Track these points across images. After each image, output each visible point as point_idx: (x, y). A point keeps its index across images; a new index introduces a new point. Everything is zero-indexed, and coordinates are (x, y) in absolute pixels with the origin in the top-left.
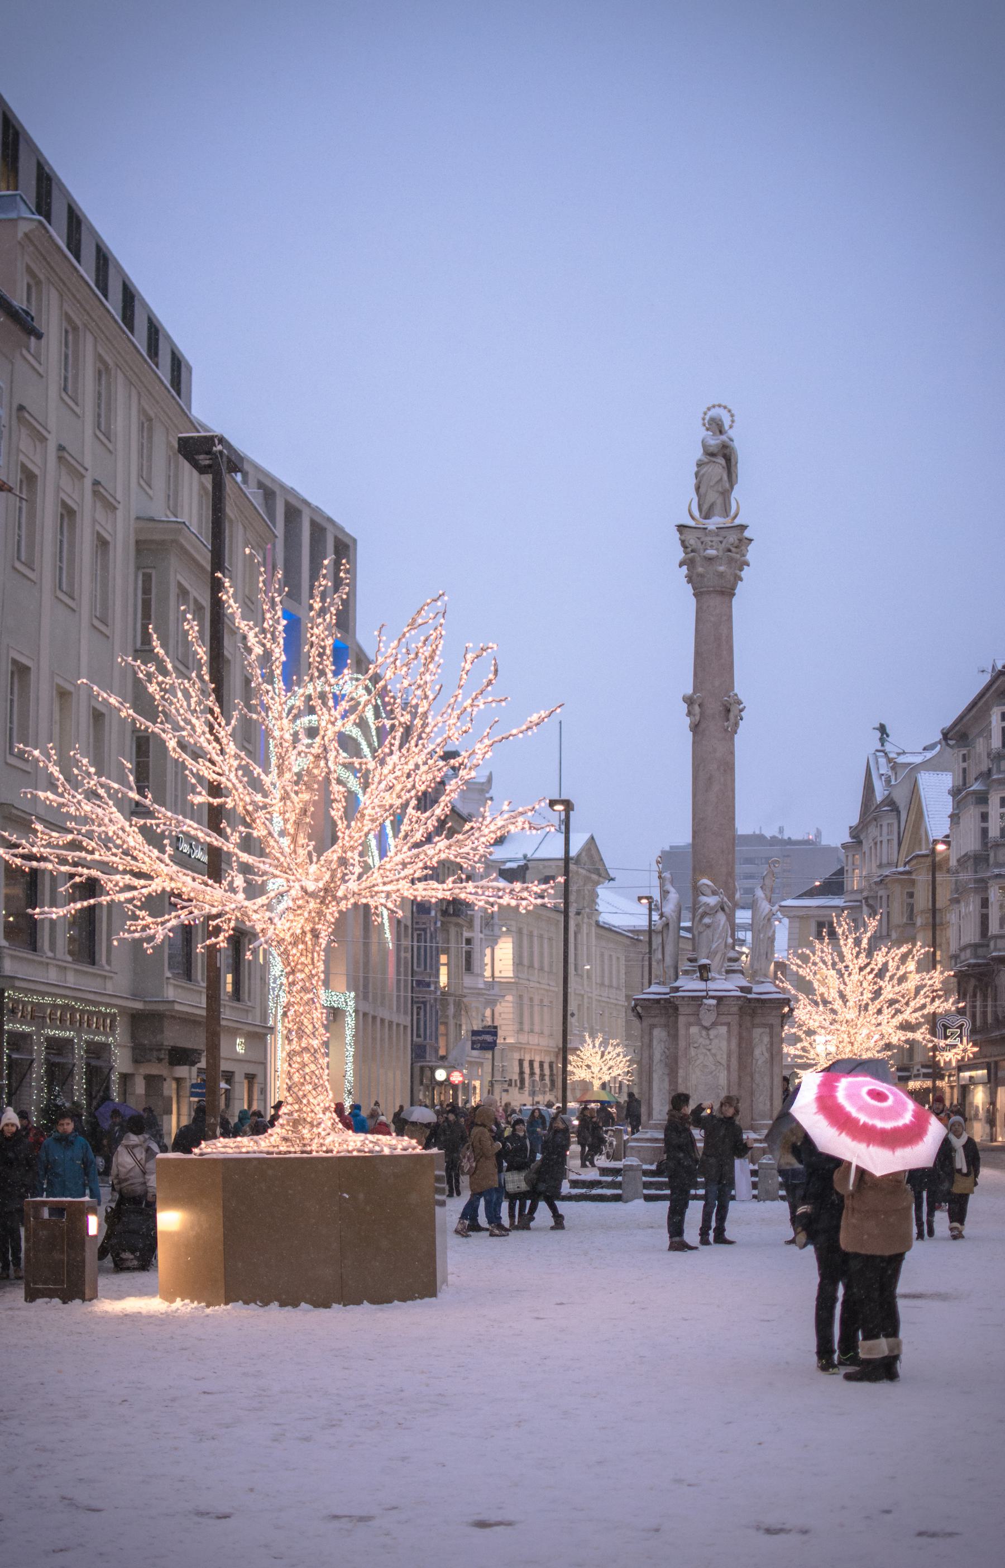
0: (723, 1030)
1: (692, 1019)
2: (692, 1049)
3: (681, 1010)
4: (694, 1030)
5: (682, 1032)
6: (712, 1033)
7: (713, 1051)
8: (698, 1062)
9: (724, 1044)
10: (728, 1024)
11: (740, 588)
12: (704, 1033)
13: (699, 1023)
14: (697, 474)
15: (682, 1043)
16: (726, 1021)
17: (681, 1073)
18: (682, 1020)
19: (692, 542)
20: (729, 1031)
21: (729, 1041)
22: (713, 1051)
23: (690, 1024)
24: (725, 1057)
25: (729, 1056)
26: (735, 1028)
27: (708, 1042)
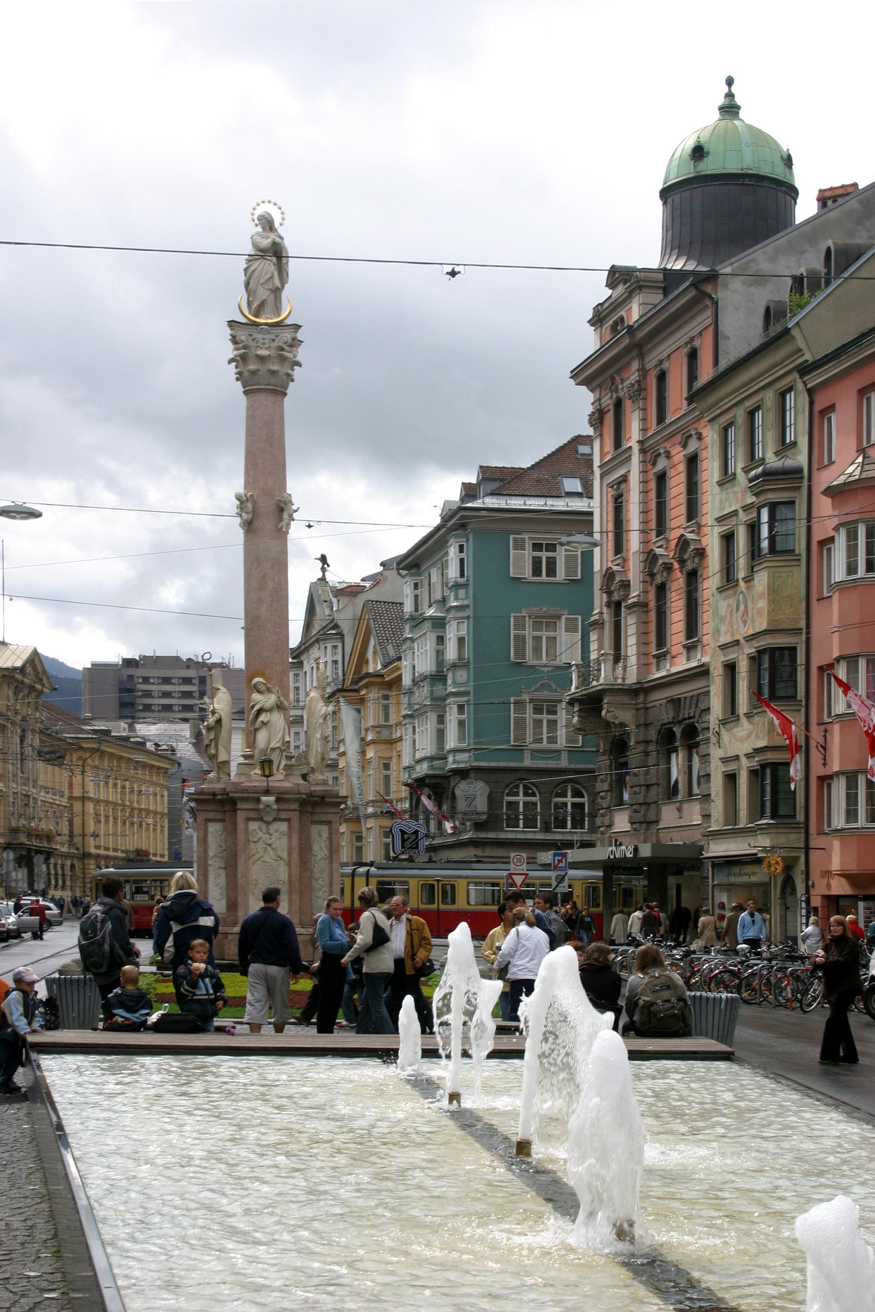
0: (284, 826)
1: (252, 815)
2: (252, 845)
3: (239, 806)
4: (253, 826)
5: (241, 826)
9: (285, 840)
10: (288, 820)
12: (264, 827)
13: (261, 819)
15: (241, 837)
17: (241, 869)
18: (241, 816)
20: (290, 828)
21: (290, 838)
23: (249, 819)
25: (290, 854)
26: (296, 824)
27: (267, 836)
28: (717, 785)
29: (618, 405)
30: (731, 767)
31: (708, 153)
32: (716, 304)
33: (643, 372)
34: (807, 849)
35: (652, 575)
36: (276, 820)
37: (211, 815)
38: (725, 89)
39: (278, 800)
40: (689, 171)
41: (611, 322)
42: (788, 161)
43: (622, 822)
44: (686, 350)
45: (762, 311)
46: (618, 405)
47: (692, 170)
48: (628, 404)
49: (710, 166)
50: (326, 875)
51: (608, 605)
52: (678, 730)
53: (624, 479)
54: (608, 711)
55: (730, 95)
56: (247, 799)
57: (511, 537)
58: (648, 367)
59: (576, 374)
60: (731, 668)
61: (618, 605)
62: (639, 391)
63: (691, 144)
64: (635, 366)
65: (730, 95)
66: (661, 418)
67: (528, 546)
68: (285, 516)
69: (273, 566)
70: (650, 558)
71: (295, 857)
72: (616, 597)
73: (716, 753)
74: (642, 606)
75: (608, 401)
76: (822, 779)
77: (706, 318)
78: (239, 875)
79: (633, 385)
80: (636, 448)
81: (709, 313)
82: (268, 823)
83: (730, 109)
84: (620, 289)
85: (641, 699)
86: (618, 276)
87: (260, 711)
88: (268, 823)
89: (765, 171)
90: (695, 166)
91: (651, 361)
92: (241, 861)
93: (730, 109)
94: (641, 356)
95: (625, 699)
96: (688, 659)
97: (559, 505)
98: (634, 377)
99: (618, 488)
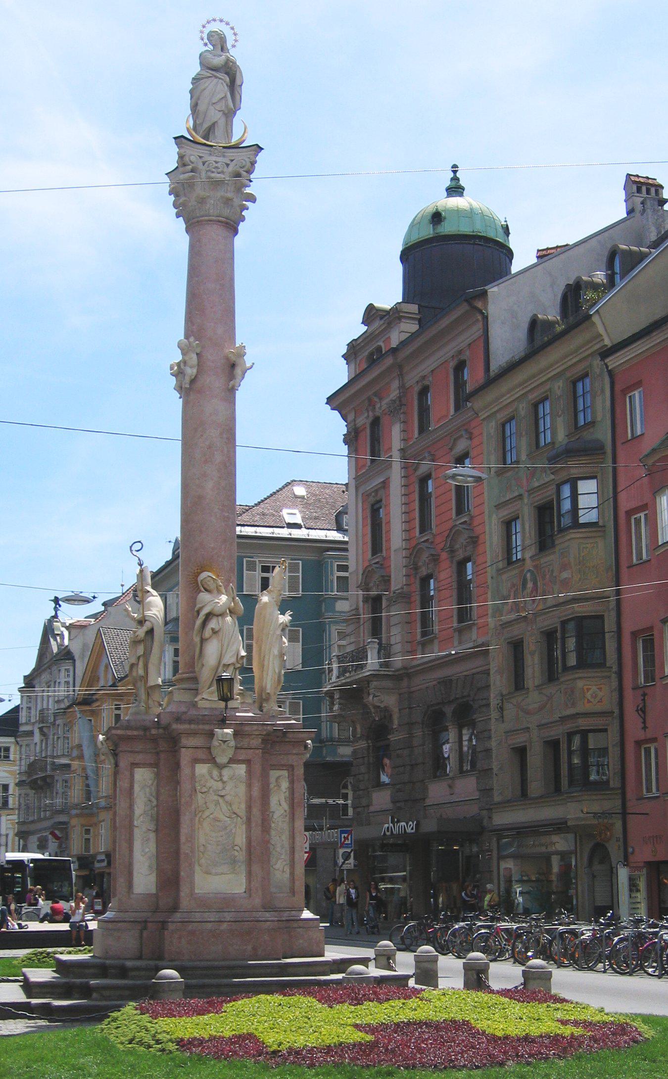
0: (241, 769)
1: (201, 754)
2: (199, 795)
3: (184, 741)
4: (202, 769)
5: (185, 771)
6: (226, 773)
7: (228, 798)
8: (207, 813)
9: (242, 789)
10: (248, 762)
11: (242, 227)
12: (215, 773)
13: (212, 760)
14: (191, 92)
15: (186, 786)
16: (248, 757)
17: (184, 830)
18: (185, 756)
19: (193, 158)
20: (249, 772)
21: (249, 786)
22: (228, 798)
23: (196, 761)
24: (243, 806)
25: (249, 808)
26: (257, 768)
27: (220, 784)
28: (500, 759)
29: (376, 423)
30: (520, 739)
31: (445, 218)
32: (486, 318)
33: (404, 390)
34: (624, 814)
35: (416, 568)
36: (232, 761)
37: (139, 758)
38: (452, 175)
39: (236, 734)
40: (428, 232)
41: (366, 353)
42: (506, 230)
43: (381, 799)
44: (452, 364)
45: (525, 326)
46: (376, 423)
47: (432, 232)
48: (384, 421)
49: (447, 228)
50: (285, 837)
51: (366, 599)
52: (448, 710)
53: (385, 484)
54: (374, 696)
55: (455, 179)
56: (194, 734)
57: (245, 560)
58: (407, 385)
59: (330, 400)
60: (517, 647)
61: (377, 600)
62: (399, 405)
63: (431, 210)
64: (396, 384)
65: (455, 179)
66: (422, 429)
67: (259, 568)
68: (238, 371)
69: (221, 434)
70: (413, 553)
71: (256, 811)
72: (374, 593)
73: (497, 729)
74: (404, 597)
75: (363, 420)
76: (638, 743)
77: (475, 331)
78: (183, 839)
79: (394, 401)
80: (396, 457)
81: (480, 325)
82: (221, 767)
83: (455, 189)
84: (377, 324)
85: (405, 683)
86: (371, 314)
87: (209, 616)
88: (221, 767)
89: (491, 235)
90: (434, 229)
91: (412, 378)
92: (185, 820)
93: (455, 189)
94: (401, 376)
95: (388, 684)
96: (460, 643)
97: (284, 533)
98: (394, 394)
99: (376, 495)
